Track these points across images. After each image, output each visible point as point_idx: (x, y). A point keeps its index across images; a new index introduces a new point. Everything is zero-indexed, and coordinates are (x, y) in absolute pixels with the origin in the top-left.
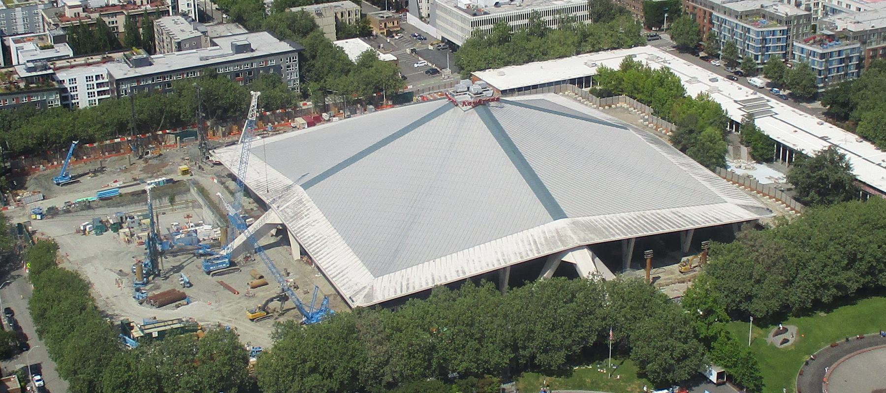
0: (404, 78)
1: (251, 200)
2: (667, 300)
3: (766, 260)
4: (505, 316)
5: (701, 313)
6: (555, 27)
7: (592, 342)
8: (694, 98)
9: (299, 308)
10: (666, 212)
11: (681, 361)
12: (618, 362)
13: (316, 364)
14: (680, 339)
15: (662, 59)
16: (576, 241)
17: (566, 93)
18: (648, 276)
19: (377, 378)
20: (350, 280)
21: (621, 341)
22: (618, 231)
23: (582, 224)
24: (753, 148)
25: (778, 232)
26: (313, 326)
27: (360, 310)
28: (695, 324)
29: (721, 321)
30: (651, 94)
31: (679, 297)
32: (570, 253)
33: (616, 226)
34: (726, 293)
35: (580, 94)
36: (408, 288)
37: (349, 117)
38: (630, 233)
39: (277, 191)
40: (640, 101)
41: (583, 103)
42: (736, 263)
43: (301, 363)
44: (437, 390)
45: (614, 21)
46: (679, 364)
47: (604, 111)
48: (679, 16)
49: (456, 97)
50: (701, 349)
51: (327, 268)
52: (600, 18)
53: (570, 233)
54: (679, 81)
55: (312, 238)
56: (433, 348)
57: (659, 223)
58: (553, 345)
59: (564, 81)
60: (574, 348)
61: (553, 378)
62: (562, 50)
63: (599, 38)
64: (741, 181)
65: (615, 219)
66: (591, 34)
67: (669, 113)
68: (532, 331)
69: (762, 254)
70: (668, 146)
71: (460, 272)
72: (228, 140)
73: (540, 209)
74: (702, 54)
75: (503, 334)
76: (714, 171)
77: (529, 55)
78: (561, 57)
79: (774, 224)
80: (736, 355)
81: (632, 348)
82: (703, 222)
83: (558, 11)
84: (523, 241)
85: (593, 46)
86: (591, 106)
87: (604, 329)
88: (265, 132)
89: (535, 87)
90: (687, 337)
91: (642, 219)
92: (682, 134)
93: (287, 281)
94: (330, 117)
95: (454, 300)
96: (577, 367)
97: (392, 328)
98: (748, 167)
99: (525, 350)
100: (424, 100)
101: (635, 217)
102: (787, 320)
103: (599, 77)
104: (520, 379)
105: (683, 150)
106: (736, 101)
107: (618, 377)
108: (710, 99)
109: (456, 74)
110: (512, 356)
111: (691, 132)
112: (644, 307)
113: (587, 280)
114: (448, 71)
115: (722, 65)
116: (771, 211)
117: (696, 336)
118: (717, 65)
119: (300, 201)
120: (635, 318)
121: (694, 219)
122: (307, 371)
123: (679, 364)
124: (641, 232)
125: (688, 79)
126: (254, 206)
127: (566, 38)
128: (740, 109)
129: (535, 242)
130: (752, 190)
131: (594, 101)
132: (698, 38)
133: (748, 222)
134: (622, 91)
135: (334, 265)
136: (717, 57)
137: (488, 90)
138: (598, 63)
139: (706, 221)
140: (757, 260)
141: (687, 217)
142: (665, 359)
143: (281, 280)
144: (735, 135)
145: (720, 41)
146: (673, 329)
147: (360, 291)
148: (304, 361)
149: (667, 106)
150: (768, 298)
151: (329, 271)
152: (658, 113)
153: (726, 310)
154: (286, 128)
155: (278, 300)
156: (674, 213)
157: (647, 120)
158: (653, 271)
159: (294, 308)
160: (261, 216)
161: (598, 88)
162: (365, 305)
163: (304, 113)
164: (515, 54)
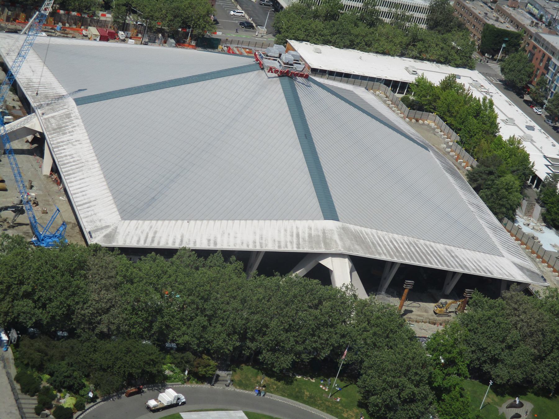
0: (216, 22)
1: (16, 98)
2: (413, 337)
3: (525, 328)
4: (243, 301)
5: (443, 361)
6: (387, 20)
7: (324, 356)
8: (504, 139)
9: (33, 227)
10: (440, 247)
11: (407, 403)
12: (343, 384)
13: (33, 289)
14: (413, 381)
15: (485, 89)
16: (340, 248)
17: (378, 92)
18: (401, 306)
19: (92, 324)
20: (95, 214)
21: (353, 363)
22: (385, 251)
23: (352, 232)
24: (548, 210)
25: (546, 303)
26: (42, 250)
27: (97, 248)
28: (433, 370)
29: (459, 375)
30: (463, 122)
31: (425, 338)
32: (330, 258)
33: (385, 246)
34: (473, 348)
35: (391, 98)
36: (153, 241)
37: (146, 44)
38: (397, 257)
39: (46, 97)
40: (450, 125)
41: (391, 108)
42: (494, 321)
43: (17, 284)
44: (150, 355)
45: (449, 34)
46: (403, 405)
47: (409, 123)
48: (517, 50)
49: (265, 60)
50: (431, 397)
51: (75, 194)
52: (436, 26)
53: (336, 237)
54: (496, 117)
55: (68, 157)
56: (159, 311)
57: (431, 256)
58: (283, 347)
59: (379, 80)
60: (303, 356)
61: (272, 380)
62: (388, 46)
63: (429, 46)
64: (525, 240)
65: (386, 238)
66: (422, 40)
67: (474, 147)
68: (267, 326)
69: (522, 320)
70: (463, 180)
71: (212, 242)
72: (11, 26)
73: (314, 202)
74: (527, 97)
75: (235, 319)
76: (501, 220)
77: (351, 41)
78: (384, 53)
79: (545, 293)
80: (464, 414)
81: (362, 375)
82: (473, 269)
83: (397, 6)
84: (286, 230)
85: (420, 53)
86: (398, 114)
87: (340, 346)
88: (53, 31)
89: (348, 76)
90: (420, 381)
91: (414, 247)
92: (481, 173)
93: (28, 194)
94: (127, 37)
95: (197, 268)
96: (300, 377)
97: (125, 276)
98: (536, 227)
99: (252, 343)
100: (230, 52)
101: (407, 242)
102: (525, 395)
103: (416, 86)
104: (238, 371)
105: (477, 189)
106: (545, 157)
107: (338, 400)
108: (521, 146)
109: (271, 35)
110: (238, 344)
111: (491, 173)
112: (387, 337)
113: (339, 291)
114: (262, 30)
115: (543, 115)
116: (545, 280)
117: (430, 383)
118: (539, 113)
119: (68, 116)
120: (375, 345)
121: (465, 263)
122: (21, 293)
123: (403, 405)
124: (408, 259)
125: (505, 118)
126: (18, 104)
127: (395, 36)
128: (547, 166)
129: (298, 235)
130: (533, 252)
131: (402, 111)
132: (528, 80)
133: (519, 283)
134: (434, 109)
135: (84, 193)
136: (541, 105)
137: (300, 64)
138: (420, 73)
139: (477, 269)
140: (515, 325)
141: (459, 259)
142: (392, 396)
143: (23, 191)
144: (533, 191)
145: (550, 90)
146: (409, 368)
147: (102, 228)
148: (21, 283)
149: (474, 139)
150: (513, 367)
151: (76, 197)
152: (464, 143)
153: (468, 366)
154: (77, 34)
155: (12, 211)
156: (447, 251)
157: (450, 147)
158: (408, 303)
159: (27, 225)
160: (22, 117)
161: (411, 98)
162: (104, 244)
163: (99, 24)
164: (338, 35)
